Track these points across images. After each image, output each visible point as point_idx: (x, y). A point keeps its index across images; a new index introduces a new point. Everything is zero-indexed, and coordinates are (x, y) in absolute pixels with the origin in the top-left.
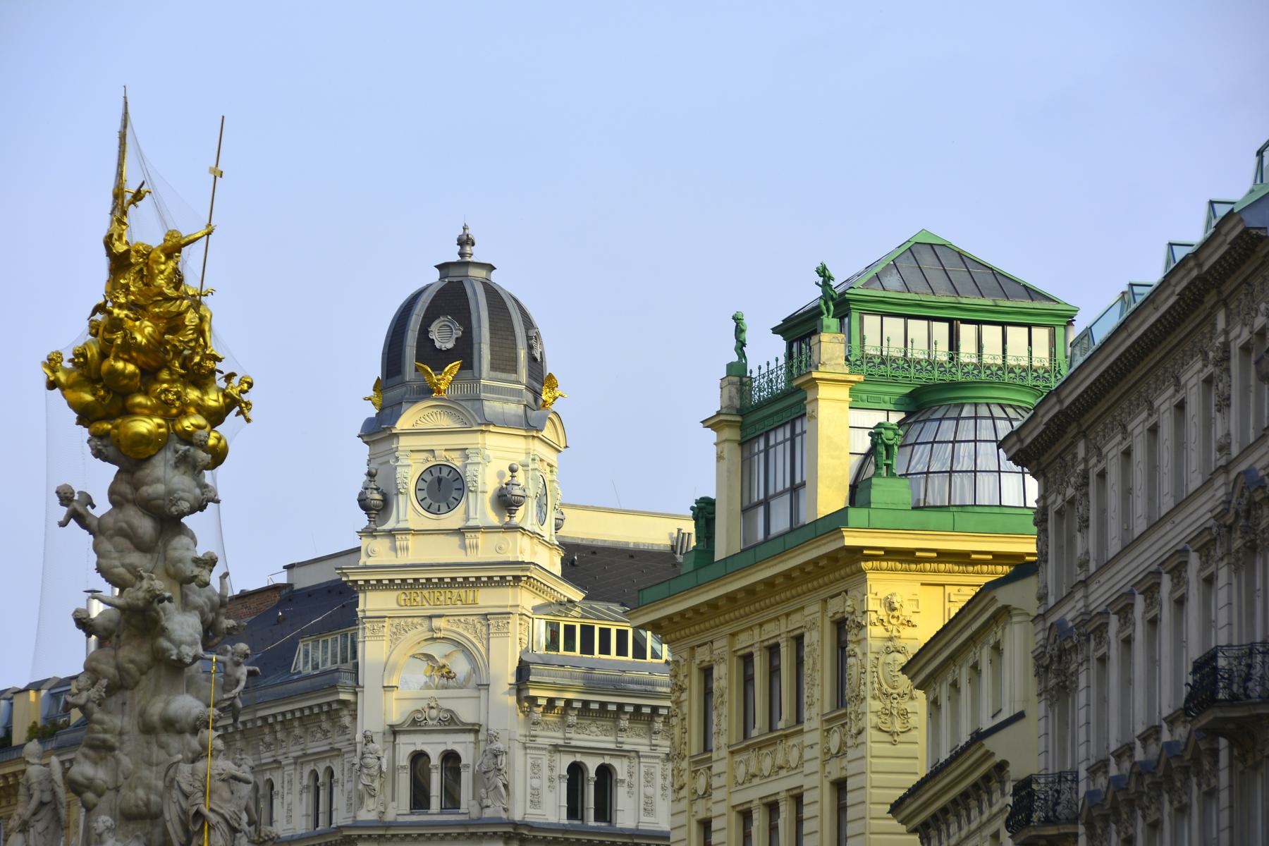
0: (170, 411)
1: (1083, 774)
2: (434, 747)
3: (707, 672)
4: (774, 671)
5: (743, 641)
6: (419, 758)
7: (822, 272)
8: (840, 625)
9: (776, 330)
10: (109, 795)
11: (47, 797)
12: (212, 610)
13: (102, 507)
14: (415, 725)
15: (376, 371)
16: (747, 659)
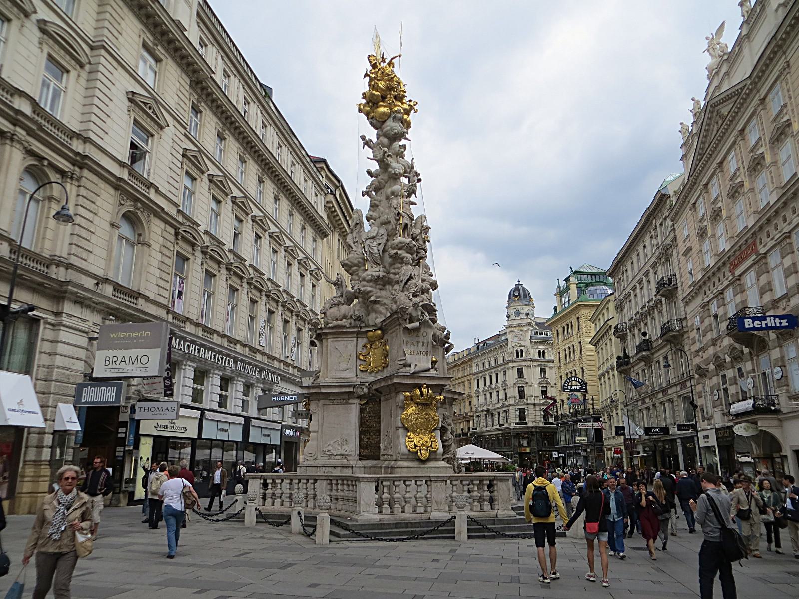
0: (390, 106)
1: (627, 322)
4: (568, 328)
6: (517, 352)
8: (578, 319)
10: (377, 220)
11: (358, 222)
12: (409, 167)
13: (374, 140)
14: (516, 346)
16: (564, 328)
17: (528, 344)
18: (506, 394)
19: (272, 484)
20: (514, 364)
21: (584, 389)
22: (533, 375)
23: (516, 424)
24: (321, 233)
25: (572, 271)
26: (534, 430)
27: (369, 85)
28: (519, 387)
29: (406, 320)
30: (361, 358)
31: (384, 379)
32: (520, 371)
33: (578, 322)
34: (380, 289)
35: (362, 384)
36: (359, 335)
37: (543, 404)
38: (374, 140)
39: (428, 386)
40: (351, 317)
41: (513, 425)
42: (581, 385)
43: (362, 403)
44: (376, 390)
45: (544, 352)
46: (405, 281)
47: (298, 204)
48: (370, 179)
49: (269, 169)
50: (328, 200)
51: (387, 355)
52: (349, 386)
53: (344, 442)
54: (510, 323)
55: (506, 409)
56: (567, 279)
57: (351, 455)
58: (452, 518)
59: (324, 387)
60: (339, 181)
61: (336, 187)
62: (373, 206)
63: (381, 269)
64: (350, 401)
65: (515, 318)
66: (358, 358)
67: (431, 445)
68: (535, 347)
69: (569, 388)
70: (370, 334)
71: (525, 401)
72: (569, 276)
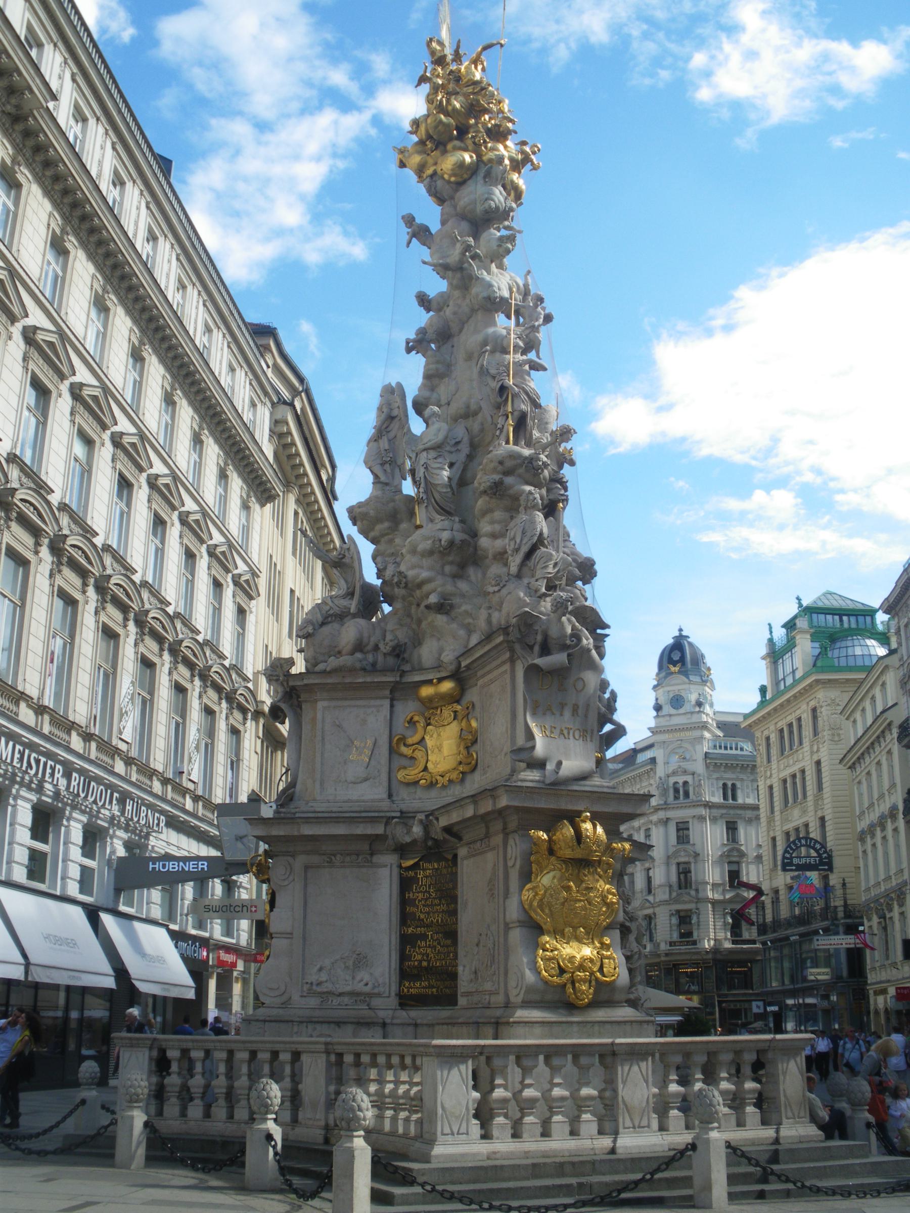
2: (681, 780)
3: (768, 739)
4: (791, 732)
5: (780, 725)
7: (798, 599)
8: (814, 710)
9: (783, 626)
14: (674, 773)
15: (656, 670)
16: (782, 731)
17: (699, 767)
18: (649, 880)
19: (179, 1061)
20: (671, 814)
21: (825, 863)
22: (710, 838)
23: (672, 944)
24: (260, 490)
25: (800, 605)
26: (710, 956)
27: (430, 100)
28: (678, 864)
29: (531, 647)
30: (404, 750)
31: (474, 798)
32: (682, 829)
33: (815, 718)
34: (455, 576)
35: (405, 817)
36: (400, 691)
37: (730, 901)
38: (435, 226)
39: (595, 818)
40: (376, 648)
41: (663, 947)
42: (820, 855)
43: (410, 863)
44: (448, 830)
45: (734, 785)
46: (525, 549)
47: (215, 418)
48: (422, 318)
49: (157, 331)
50: (278, 416)
51: (475, 742)
52: (373, 820)
53: (360, 962)
54: (663, 722)
55: (649, 911)
56: (790, 626)
57: (379, 995)
58: (686, 1149)
59: (307, 820)
60: (301, 380)
61: (295, 393)
62: (431, 378)
63: (457, 526)
64: (377, 859)
65: (673, 711)
66: (393, 751)
67: (601, 969)
68: (715, 775)
69: (795, 861)
70: (426, 691)
71: (693, 893)
72: (795, 617)
